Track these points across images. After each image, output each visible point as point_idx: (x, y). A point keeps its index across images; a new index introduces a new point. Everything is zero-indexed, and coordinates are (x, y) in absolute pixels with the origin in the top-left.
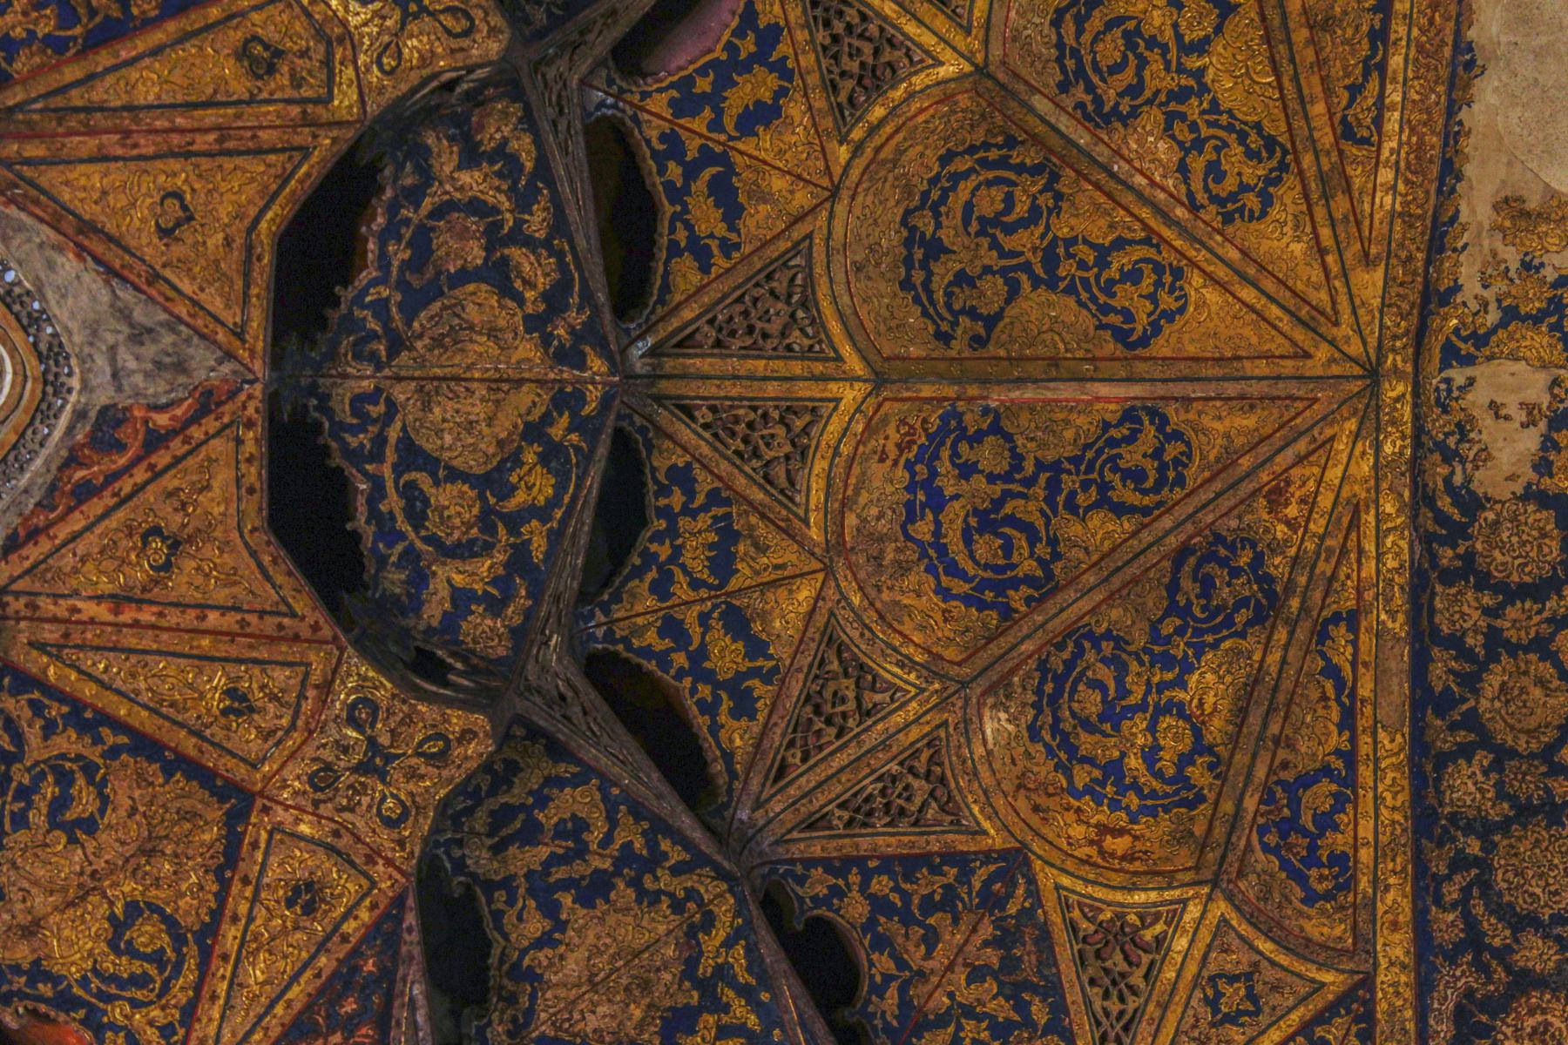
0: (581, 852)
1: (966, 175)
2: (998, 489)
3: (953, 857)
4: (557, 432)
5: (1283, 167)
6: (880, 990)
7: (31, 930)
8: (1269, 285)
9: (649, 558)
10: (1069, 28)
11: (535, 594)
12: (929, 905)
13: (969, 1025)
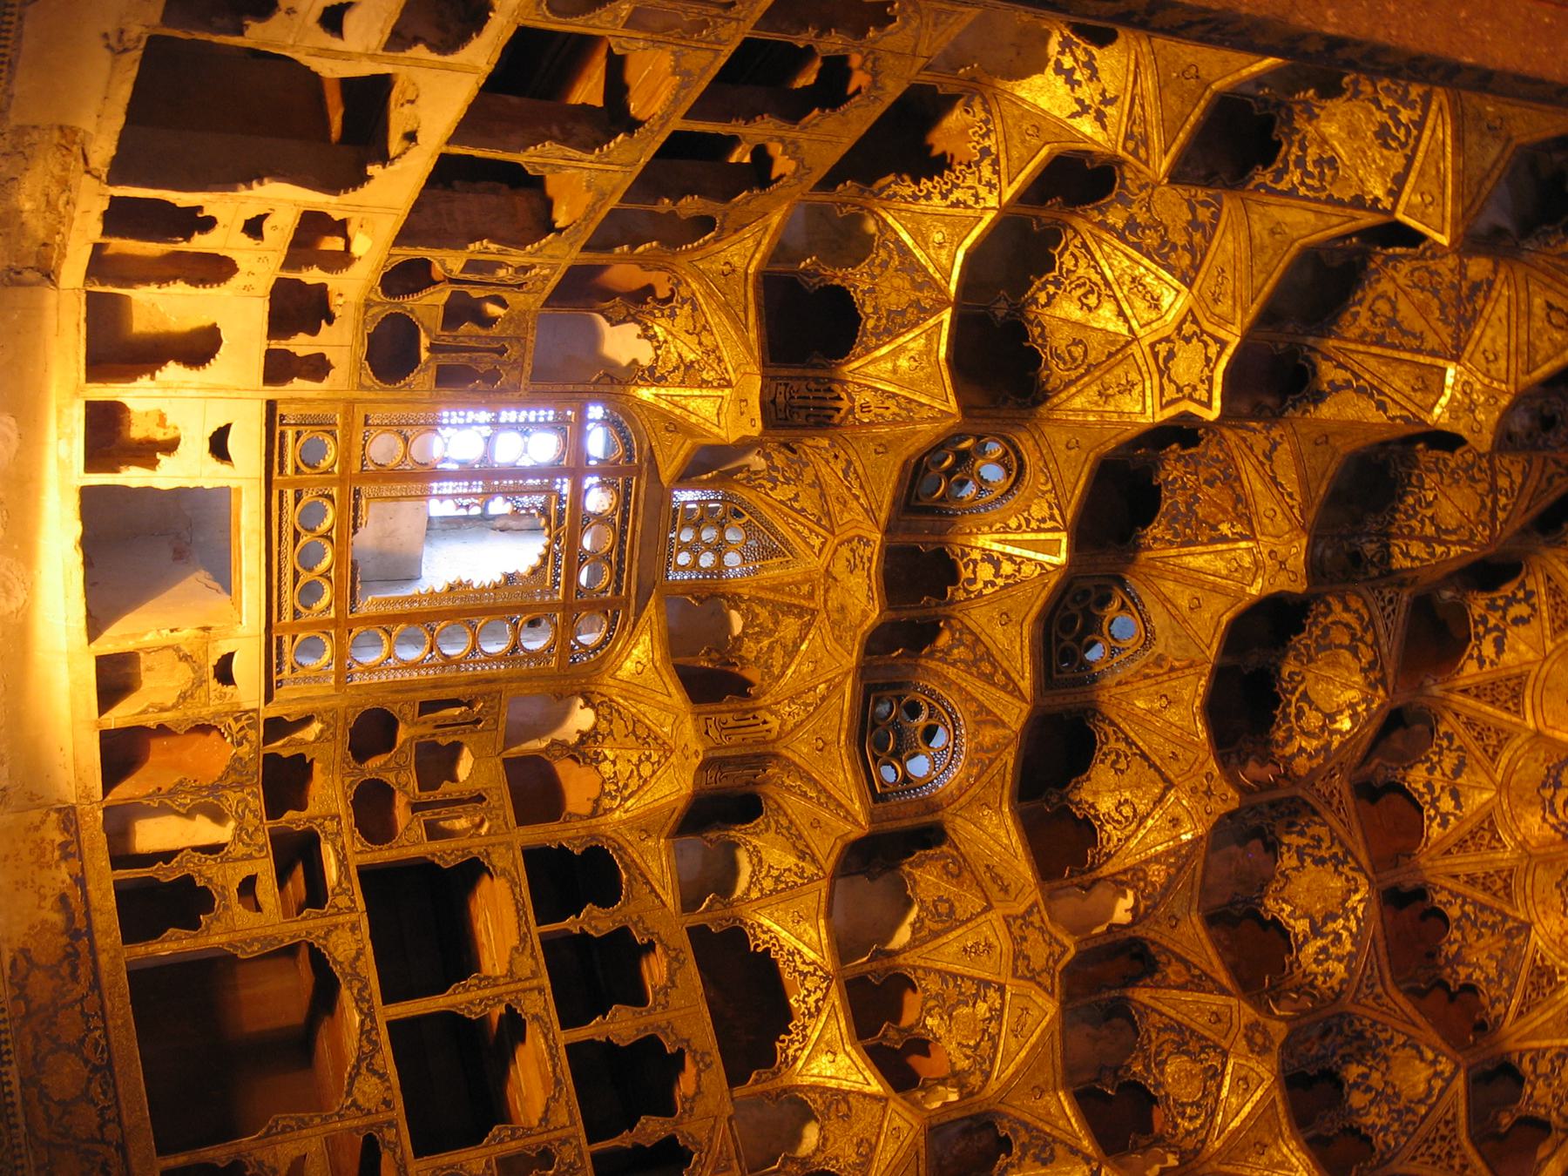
0: (1319, 847)
3: (1501, 912)
4: (1359, 709)
6: (1450, 943)
7: (1096, 793)
9: (1428, 759)
11: (1326, 760)
12: (1484, 924)
13: (1478, 972)
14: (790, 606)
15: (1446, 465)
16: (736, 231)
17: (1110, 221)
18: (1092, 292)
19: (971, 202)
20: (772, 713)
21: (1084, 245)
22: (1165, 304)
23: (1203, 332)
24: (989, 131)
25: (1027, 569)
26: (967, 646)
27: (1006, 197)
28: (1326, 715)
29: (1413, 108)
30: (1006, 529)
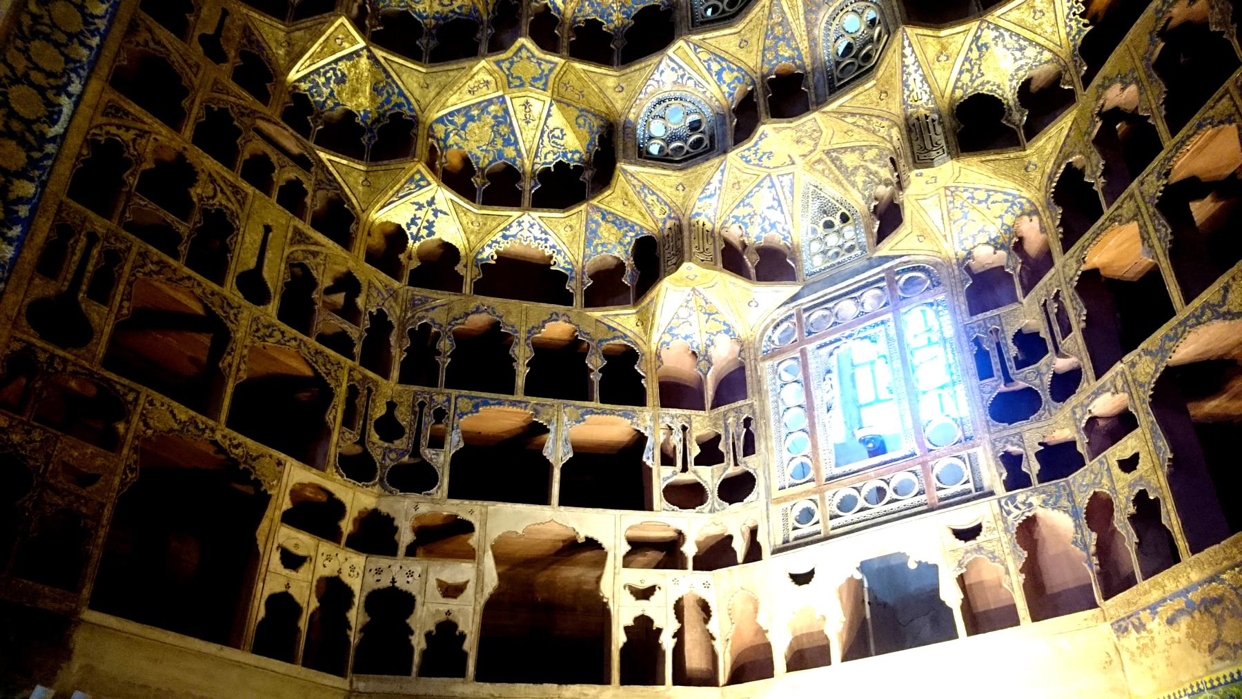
14: (839, 168)
16: (615, 330)
17: (514, 153)
18: (553, 136)
19: (536, 227)
20: (891, 138)
21: (536, 156)
22: (523, 100)
23: (508, 76)
24: (493, 242)
25: (704, 56)
26: (777, 52)
27: (519, 213)
29: (314, 80)
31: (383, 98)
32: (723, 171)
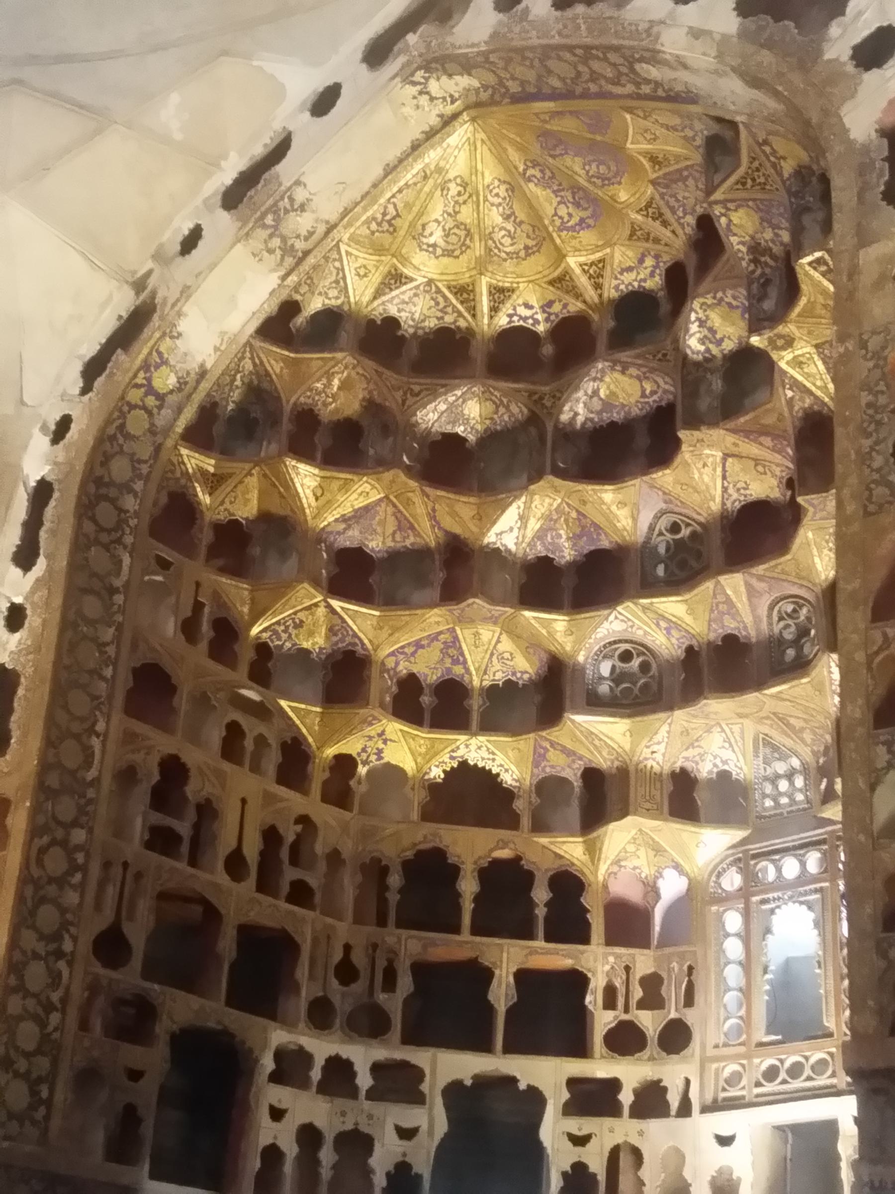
1: (505, 252)
2: (569, 205)
5: (445, 182)
8: (473, 164)
9: (639, 286)
10: (457, 253)
15: (465, 429)
17: (463, 671)
18: (503, 658)
28: (641, 381)
30: (646, 633)
31: (338, 638)
32: (670, 724)
